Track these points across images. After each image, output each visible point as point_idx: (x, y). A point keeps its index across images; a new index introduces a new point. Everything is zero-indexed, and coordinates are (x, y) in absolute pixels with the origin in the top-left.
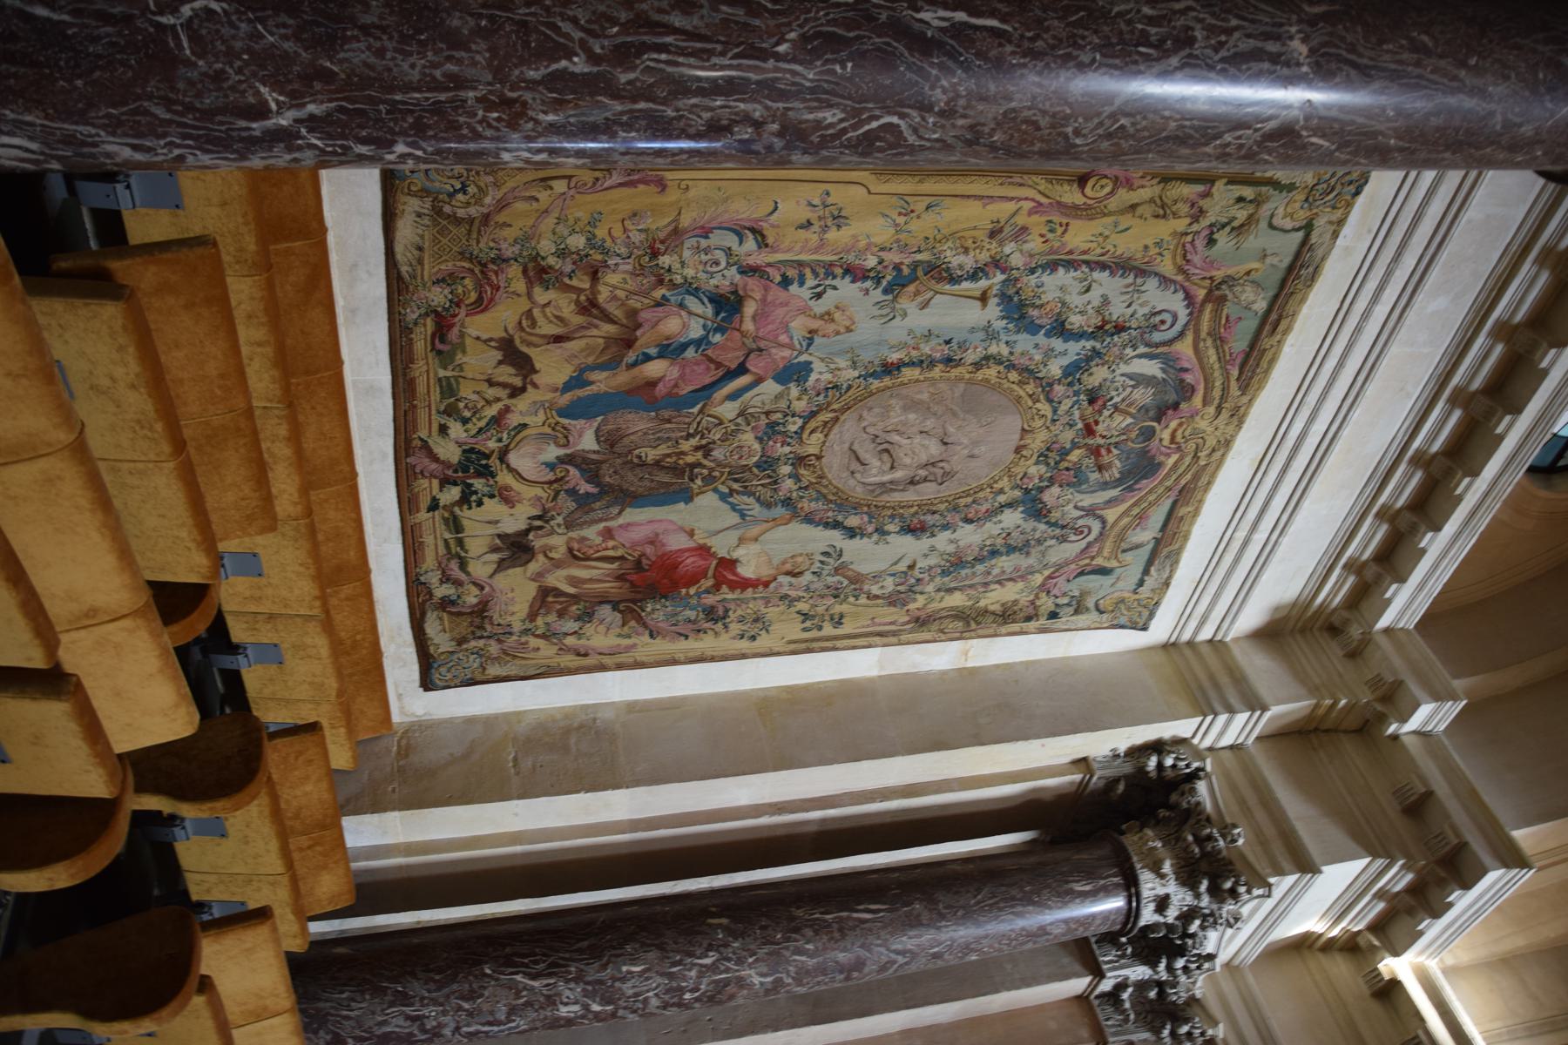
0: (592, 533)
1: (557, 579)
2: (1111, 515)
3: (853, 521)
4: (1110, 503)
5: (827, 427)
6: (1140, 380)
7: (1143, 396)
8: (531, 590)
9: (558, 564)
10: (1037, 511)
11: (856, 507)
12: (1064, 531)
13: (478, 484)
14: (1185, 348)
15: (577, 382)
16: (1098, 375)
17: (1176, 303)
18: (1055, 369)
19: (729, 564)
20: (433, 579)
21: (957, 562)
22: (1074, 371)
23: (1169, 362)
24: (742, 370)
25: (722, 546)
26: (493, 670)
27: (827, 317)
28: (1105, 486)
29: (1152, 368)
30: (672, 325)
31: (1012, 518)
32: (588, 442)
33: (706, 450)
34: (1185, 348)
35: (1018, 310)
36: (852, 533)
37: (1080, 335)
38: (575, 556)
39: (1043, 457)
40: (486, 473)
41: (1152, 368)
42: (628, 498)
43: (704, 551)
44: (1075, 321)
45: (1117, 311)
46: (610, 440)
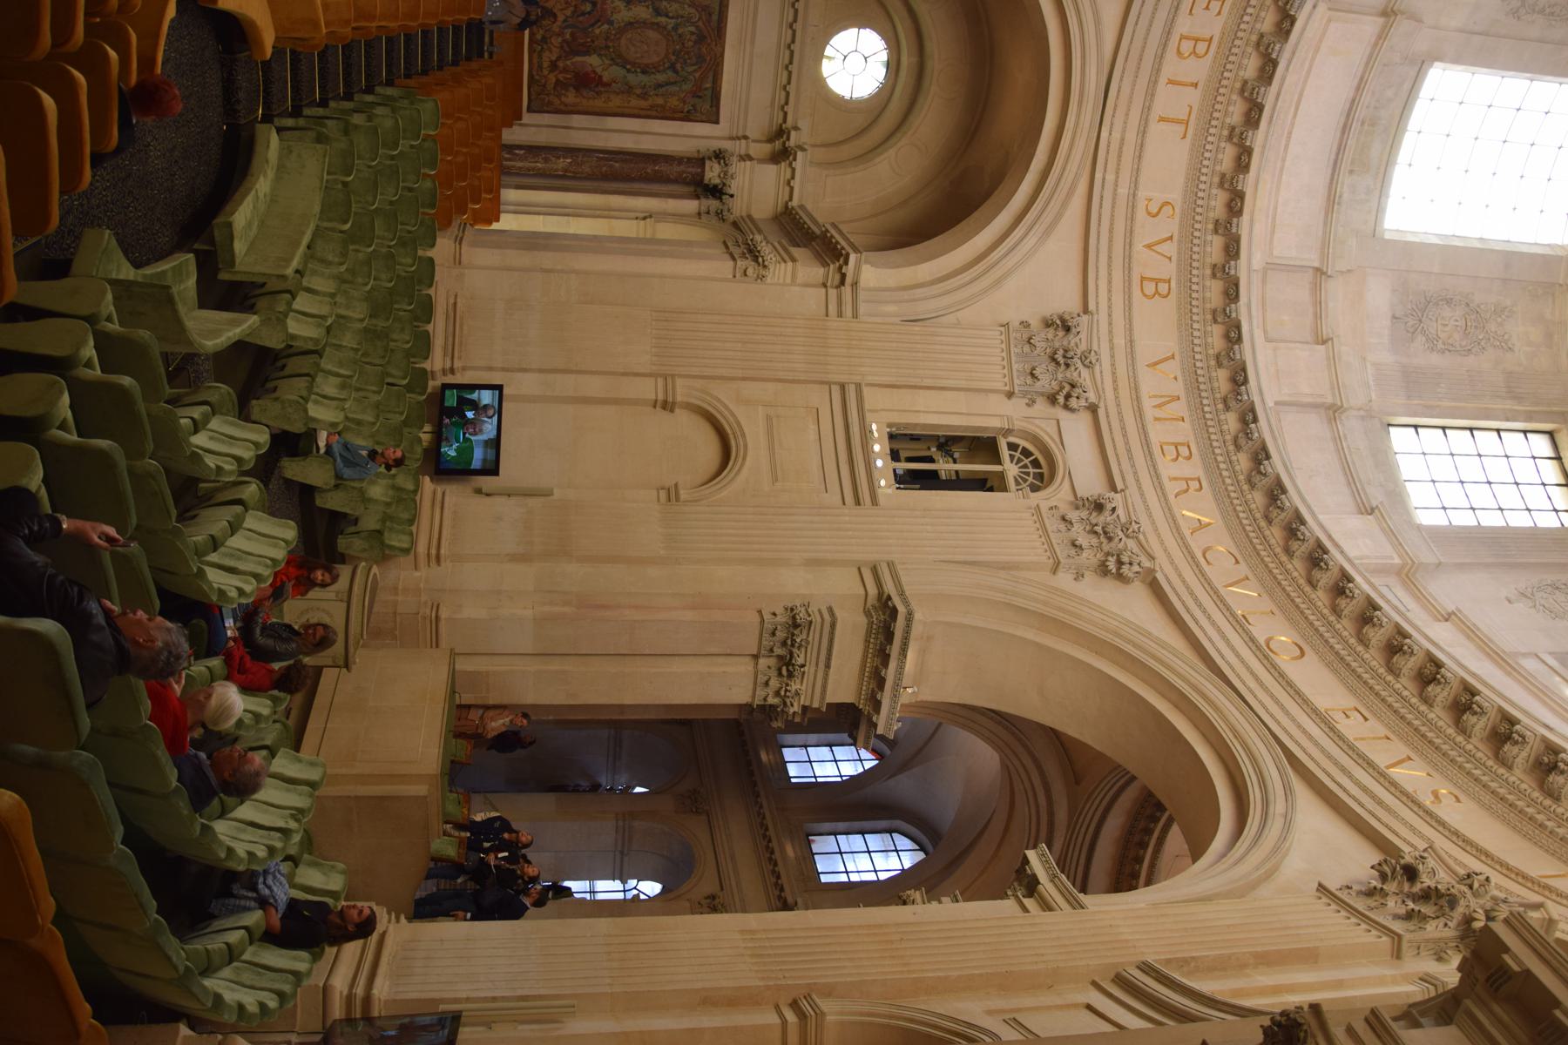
0: (568, 63)
1: (561, 77)
2: (697, 75)
3: (628, 67)
4: (695, 71)
5: (619, 38)
6: (692, 33)
7: (694, 38)
8: (554, 80)
9: (561, 72)
10: (676, 72)
11: (630, 63)
12: (685, 80)
13: (545, 46)
14: (700, 24)
15: (565, 21)
16: (680, 31)
17: (693, 11)
18: (670, 27)
19: (600, 77)
20: (535, 73)
21: (659, 86)
22: (675, 28)
23: (697, 27)
24: (599, 21)
25: (599, 70)
26: (545, 108)
27: (614, 8)
28: (693, 65)
29: (692, 29)
30: (583, 8)
31: (670, 73)
32: (568, 36)
33: (593, 41)
34: (700, 24)
35: (658, 12)
36: (628, 71)
37: (672, 18)
38: (565, 70)
39: (674, 54)
40: (546, 43)
41: (692, 29)
42: (578, 53)
43: (594, 71)
44: (671, 15)
45: (681, 12)
46: (572, 34)
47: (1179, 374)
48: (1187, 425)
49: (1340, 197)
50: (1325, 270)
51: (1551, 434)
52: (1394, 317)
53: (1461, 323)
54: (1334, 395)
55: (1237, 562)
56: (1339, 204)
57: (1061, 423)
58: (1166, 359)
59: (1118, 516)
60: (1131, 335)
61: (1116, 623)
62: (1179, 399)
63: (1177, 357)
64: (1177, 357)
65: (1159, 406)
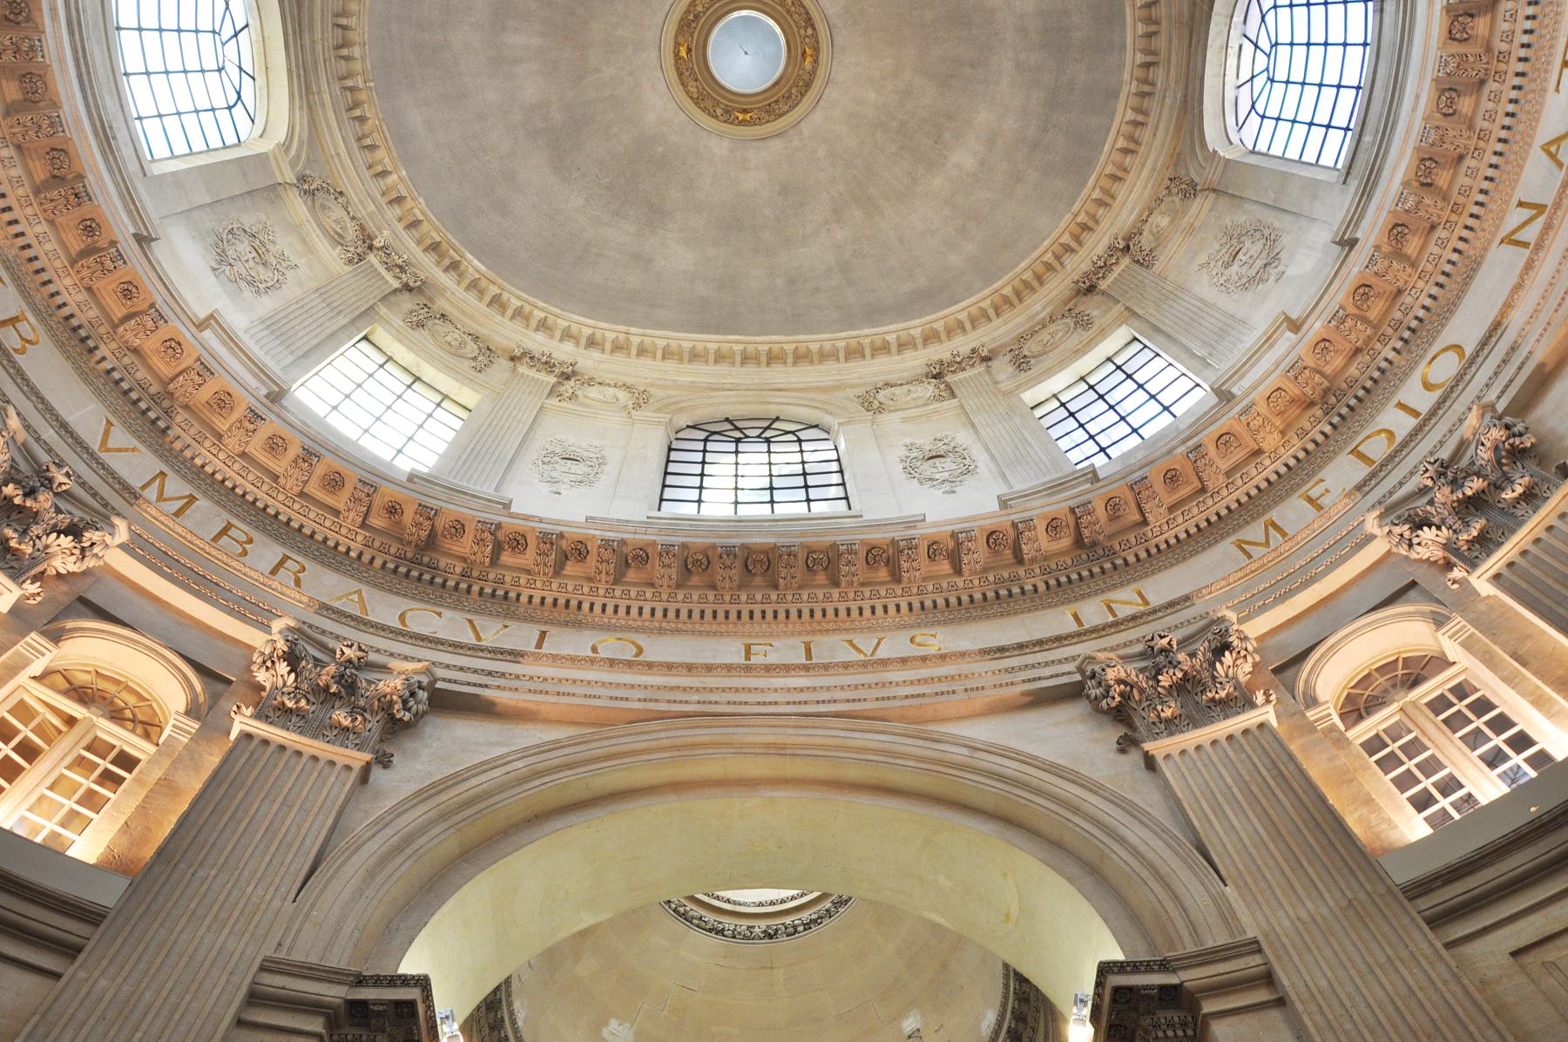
47: (134, 443)
48: (202, 503)
49: (111, 128)
50: (145, 234)
51: (365, 338)
52: (214, 270)
53: (254, 254)
54: (264, 383)
55: (439, 614)
56: (114, 138)
57: (91, 596)
58: (107, 433)
59: (315, 659)
60: (57, 418)
61: (519, 764)
62: (162, 474)
63: (113, 420)
64: (113, 420)
65: (161, 497)
